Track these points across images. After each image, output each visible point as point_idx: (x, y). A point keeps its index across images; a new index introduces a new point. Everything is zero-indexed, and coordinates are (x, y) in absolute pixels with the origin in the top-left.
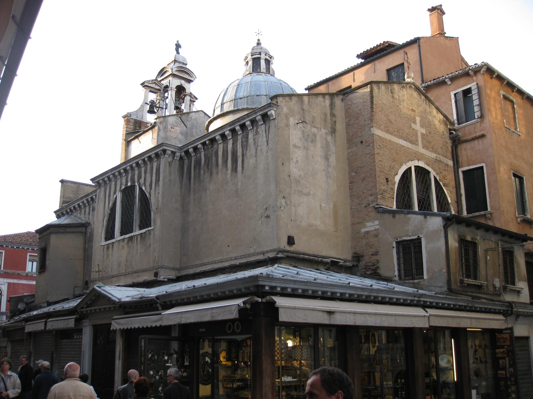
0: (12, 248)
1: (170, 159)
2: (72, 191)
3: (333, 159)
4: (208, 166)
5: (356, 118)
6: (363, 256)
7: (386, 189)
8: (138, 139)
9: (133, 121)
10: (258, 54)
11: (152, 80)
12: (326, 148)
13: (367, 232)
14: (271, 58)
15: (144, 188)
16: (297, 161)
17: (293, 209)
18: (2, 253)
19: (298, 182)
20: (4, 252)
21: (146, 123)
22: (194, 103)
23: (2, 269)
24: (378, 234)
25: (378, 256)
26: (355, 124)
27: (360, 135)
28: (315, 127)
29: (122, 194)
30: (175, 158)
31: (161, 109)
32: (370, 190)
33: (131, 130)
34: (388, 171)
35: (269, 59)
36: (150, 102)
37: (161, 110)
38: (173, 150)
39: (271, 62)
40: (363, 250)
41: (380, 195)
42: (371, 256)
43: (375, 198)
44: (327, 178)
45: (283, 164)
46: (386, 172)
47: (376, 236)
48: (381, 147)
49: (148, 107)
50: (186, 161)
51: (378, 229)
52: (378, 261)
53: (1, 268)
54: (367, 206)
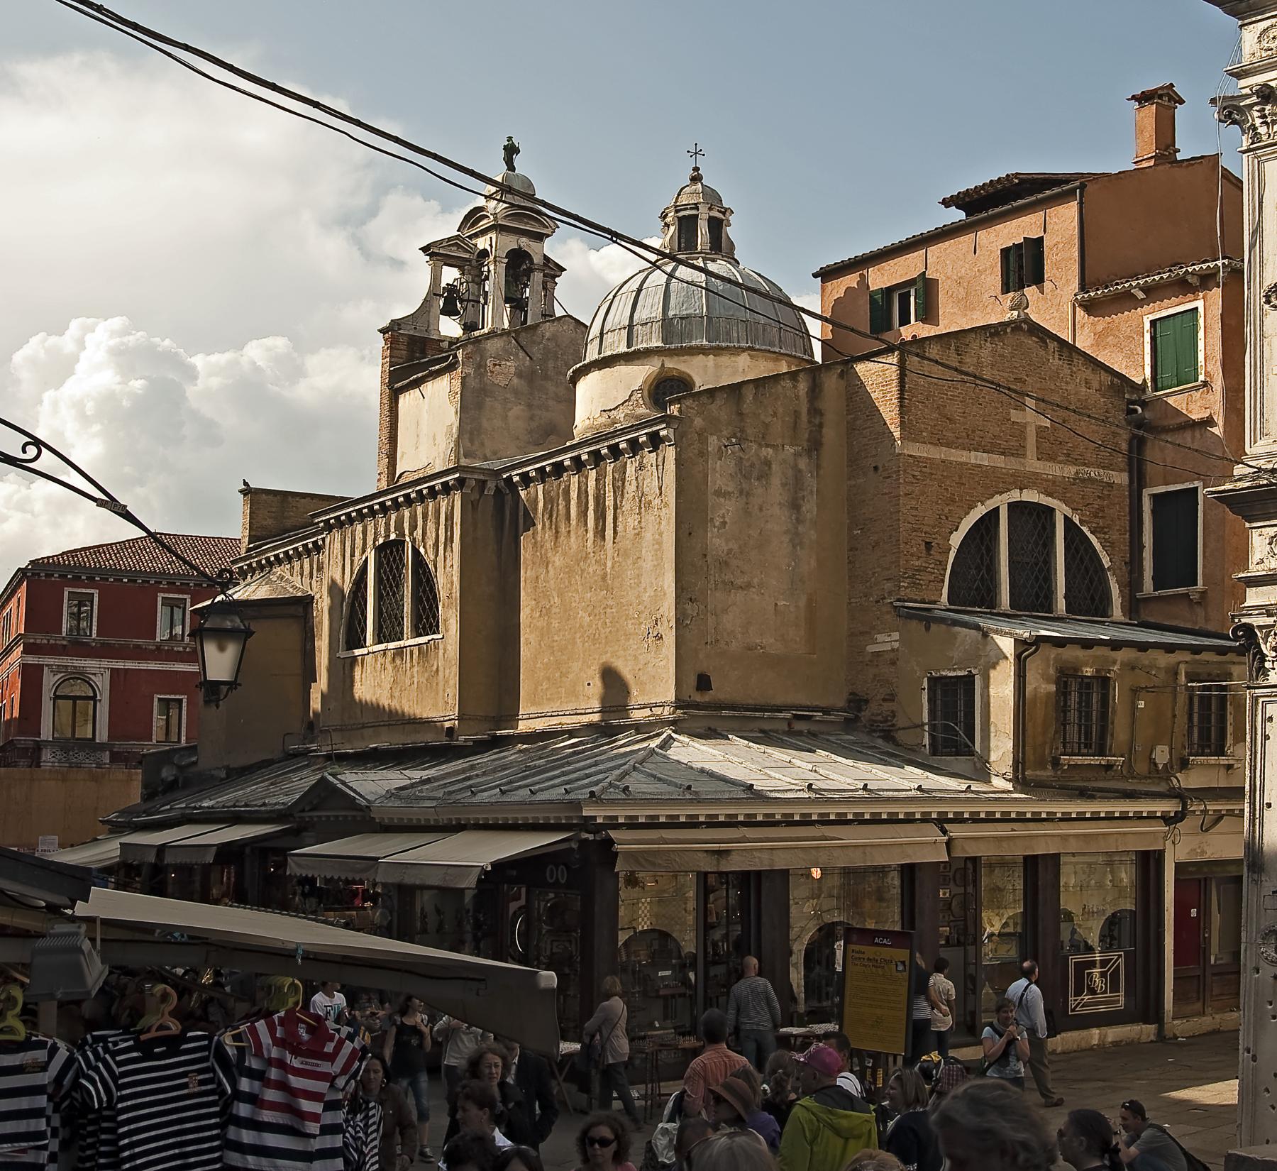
3: (810, 507)
5: (867, 416)
6: (867, 701)
7: (924, 565)
12: (796, 484)
13: (878, 654)
17: (711, 620)
19: (724, 565)
24: (898, 659)
25: (895, 704)
26: (866, 428)
27: (874, 453)
28: (767, 446)
32: (888, 569)
34: (934, 527)
40: (867, 689)
41: (907, 580)
42: (881, 702)
43: (895, 586)
44: (794, 547)
46: (926, 529)
47: (893, 663)
48: (918, 479)
51: (898, 650)
52: (894, 714)
54: (879, 602)
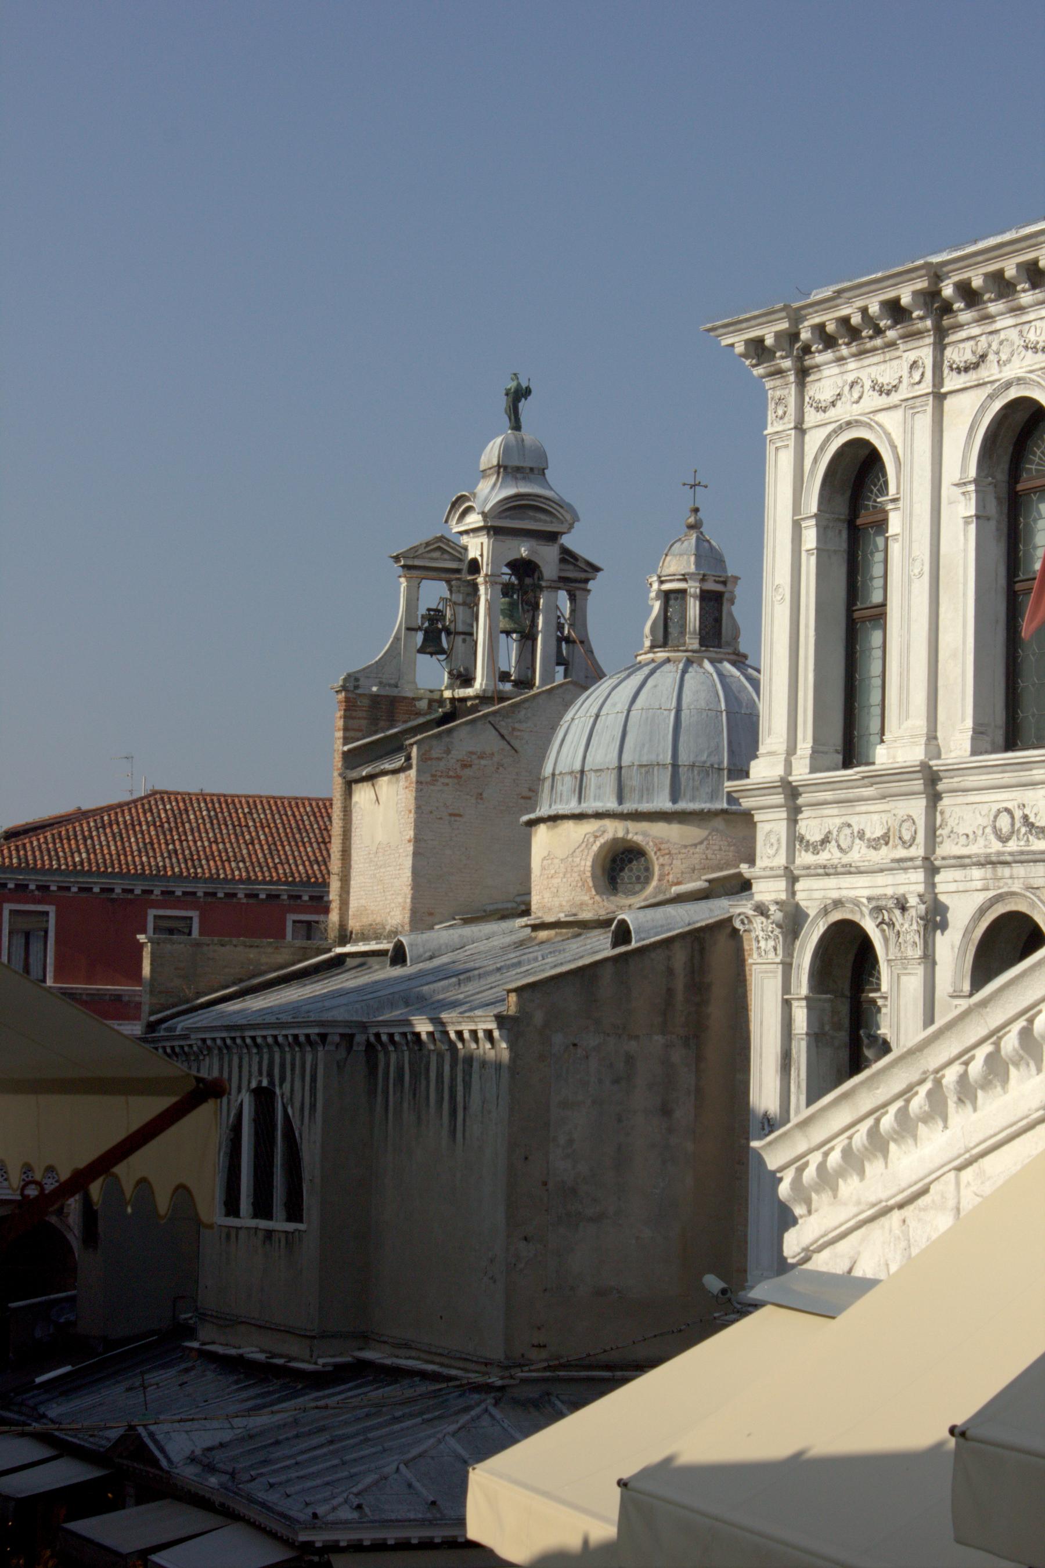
0: (84, 895)
1: (342, 1053)
2: (176, 969)
4: (415, 1094)
8: (373, 785)
9: (366, 702)
10: (679, 580)
11: (428, 544)
14: (724, 583)
15: (290, 1110)
16: (571, 1142)
18: (47, 913)
20: (51, 909)
21: (413, 699)
22: (591, 585)
23: (49, 982)
29: (256, 1101)
30: (355, 1048)
31: (462, 637)
33: (360, 734)
35: (719, 588)
36: (423, 616)
37: (464, 641)
38: (348, 1031)
39: (726, 596)
45: (526, 1158)
49: (420, 637)
50: (381, 1056)
53: (44, 981)
